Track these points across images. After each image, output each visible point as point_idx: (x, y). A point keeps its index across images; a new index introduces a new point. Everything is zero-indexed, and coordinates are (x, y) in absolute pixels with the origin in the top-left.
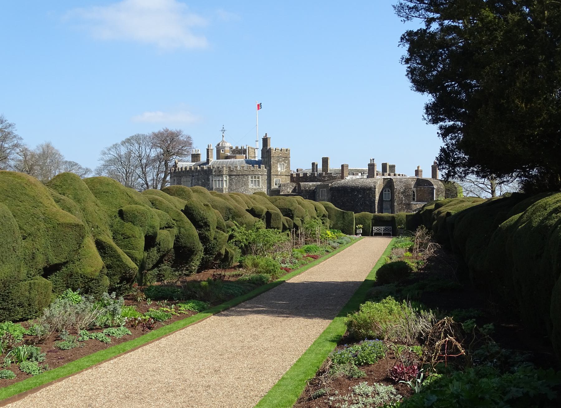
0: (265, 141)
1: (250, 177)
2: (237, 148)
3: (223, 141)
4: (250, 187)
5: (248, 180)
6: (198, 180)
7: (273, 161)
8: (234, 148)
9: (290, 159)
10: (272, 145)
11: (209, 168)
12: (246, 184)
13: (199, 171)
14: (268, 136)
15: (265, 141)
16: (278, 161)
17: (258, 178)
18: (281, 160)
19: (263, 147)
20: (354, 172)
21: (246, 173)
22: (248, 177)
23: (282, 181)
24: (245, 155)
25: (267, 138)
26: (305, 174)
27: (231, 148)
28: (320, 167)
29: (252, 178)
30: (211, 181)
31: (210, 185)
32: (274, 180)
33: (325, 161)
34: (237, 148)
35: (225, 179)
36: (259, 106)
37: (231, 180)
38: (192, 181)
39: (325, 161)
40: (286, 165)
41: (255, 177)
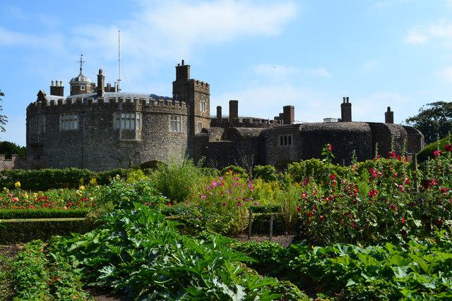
4: (170, 130)
6: (93, 118)
7: (196, 96)
9: (210, 97)
11: (112, 101)
12: (165, 127)
13: (95, 105)
22: (168, 117)
28: (226, 113)
30: (115, 121)
32: (197, 121)
33: (234, 105)
35: (138, 117)
37: (145, 120)
38: (81, 118)
39: (234, 105)
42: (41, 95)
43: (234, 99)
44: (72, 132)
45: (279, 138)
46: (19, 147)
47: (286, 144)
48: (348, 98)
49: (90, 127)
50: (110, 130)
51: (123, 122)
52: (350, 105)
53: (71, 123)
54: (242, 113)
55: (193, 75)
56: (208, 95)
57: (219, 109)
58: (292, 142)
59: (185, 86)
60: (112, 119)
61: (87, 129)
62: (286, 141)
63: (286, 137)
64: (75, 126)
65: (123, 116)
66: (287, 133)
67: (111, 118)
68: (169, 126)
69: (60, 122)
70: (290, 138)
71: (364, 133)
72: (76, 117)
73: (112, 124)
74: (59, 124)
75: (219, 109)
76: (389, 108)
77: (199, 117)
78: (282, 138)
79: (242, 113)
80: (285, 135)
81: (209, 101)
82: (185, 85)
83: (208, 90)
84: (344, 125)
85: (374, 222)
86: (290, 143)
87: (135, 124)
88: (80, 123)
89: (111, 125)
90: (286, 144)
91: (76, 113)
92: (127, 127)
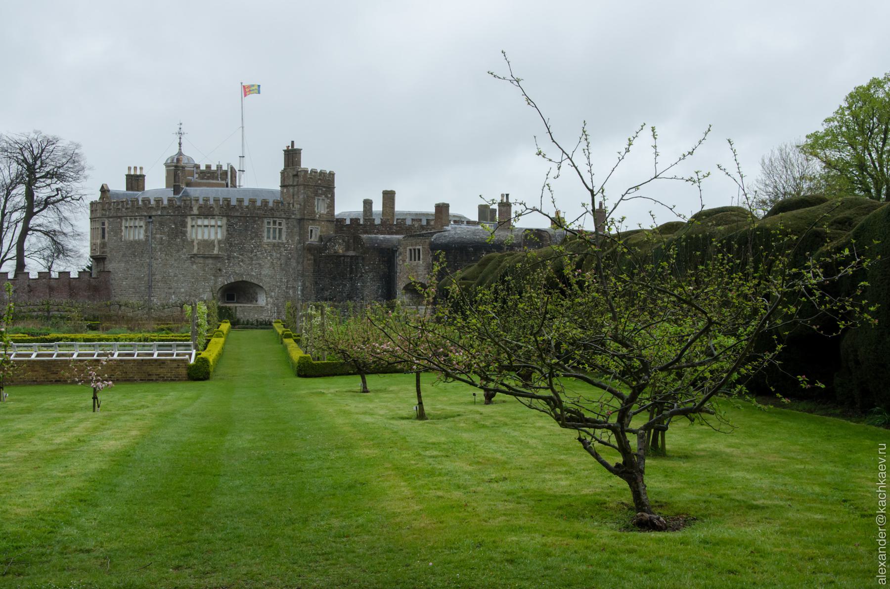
0: (292, 155)
1: (266, 221)
2: (219, 167)
3: (180, 153)
4: (265, 240)
6: (161, 224)
8: (203, 168)
9: (336, 191)
12: (257, 235)
16: (317, 194)
17: (280, 224)
18: (320, 192)
20: (459, 221)
22: (263, 222)
23: (321, 232)
24: (224, 182)
26: (355, 221)
27: (198, 167)
28: (378, 207)
29: (269, 223)
30: (189, 228)
31: (188, 235)
33: (389, 197)
34: (208, 167)
36: (247, 90)
37: (230, 226)
39: (389, 197)
44: (138, 242)
45: (408, 252)
49: (158, 236)
50: (184, 241)
53: (135, 232)
54: (402, 206)
55: (307, 163)
57: (368, 204)
60: (185, 227)
65: (200, 222)
66: (416, 245)
67: (184, 224)
68: (265, 234)
69: (123, 228)
70: (419, 250)
72: (142, 223)
73: (186, 232)
75: (368, 204)
77: (313, 220)
79: (402, 206)
85: (10, 307)
86: (419, 259)
87: (217, 233)
88: (146, 231)
89: (184, 233)
91: (141, 217)
92: (206, 237)
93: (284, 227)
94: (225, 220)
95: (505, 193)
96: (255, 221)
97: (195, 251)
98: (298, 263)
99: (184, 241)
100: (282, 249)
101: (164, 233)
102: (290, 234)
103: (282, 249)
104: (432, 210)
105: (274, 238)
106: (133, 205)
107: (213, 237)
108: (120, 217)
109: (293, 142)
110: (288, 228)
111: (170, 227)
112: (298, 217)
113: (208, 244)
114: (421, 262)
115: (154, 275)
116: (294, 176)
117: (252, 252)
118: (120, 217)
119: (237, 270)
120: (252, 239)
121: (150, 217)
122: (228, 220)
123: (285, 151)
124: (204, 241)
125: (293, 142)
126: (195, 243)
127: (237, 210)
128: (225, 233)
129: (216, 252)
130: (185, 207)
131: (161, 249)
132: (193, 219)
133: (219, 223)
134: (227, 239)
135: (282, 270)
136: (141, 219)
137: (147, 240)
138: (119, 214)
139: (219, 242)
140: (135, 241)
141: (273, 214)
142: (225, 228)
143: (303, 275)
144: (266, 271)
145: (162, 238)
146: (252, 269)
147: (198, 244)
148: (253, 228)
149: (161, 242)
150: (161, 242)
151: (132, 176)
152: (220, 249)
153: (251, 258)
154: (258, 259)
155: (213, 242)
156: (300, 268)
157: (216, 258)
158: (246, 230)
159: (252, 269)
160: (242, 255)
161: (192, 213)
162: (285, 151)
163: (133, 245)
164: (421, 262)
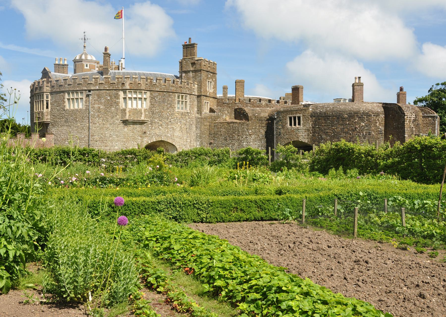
1: (177, 95)
4: (177, 110)
5: (174, 100)
6: (99, 96)
9: (218, 76)
10: (200, 54)
12: (172, 106)
14: (192, 42)
15: (189, 48)
16: (208, 78)
18: (209, 76)
19: (185, 55)
21: (173, 89)
22: (175, 96)
23: (210, 105)
25: (194, 44)
30: (121, 100)
31: (120, 105)
33: (240, 84)
37: (152, 98)
39: (240, 84)
40: (213, 83)
41: (182, 96)
42: (45, 74)
43: (239, 78)
46: (19, 125)
47: (295, 125)
48: (359, 78)
49: (96, 106)
50: (117, 109)
51: (129, 102)
52: (362, 85)
56: (214, 73)
57: (225, 88)
58: (302, 122)
59: (192, 66)
60: (118, 98)
61: (93, 107)
62: (295, 120)
63: (295, 118)
64: (80, 106)
67: (117, 97)
68: (176, 106)
69: (66, 100)
70: (299, 118)
71: (377, 114)
74: (64, 102)
76: (401, 89)
77: (206, 96)
78: (290, 118)
80: (294, 115)
81: (216, 80)
82: (192, 63)
83: (215, 69)
84: (355, 106)
86: (299, 124)
89: (118, 104)
90: (295, 125)
92: (134, 106)
93: (188, 100)
94: (148, 93)
95: (357, 76)
96: (170, 95)
97: (127, 118)
98: (197, 127)
99: (117, 109)
100: (187, 117)
101: (101, 103)
102: (192, 107)
103: (187, 117)
104: (290, 91)
105: (182, 108)
106: (75, 82)
107: (139, 107)
108: (63, 92)
109: (190, 38)
110: (190, 101)
111: (106, 99)
112: (196, 94)
113: (137, 112)
114: (302, 126)
115: (92, 136)
116: (192, 63)
117: (168, 119)
118: (63, 92)
119: (157, 131)
120: (168, 109)
121: (90, 91)
122: (151, 94)
123: (184, 46)
124: (134, 109)
125: (190, 38)
126: (127, 111)
127: (158, 87)
128: (149, 104)
129: (143, 118)
130: (118, 83)
131: (98, 116)
132: (125, 93)
133: (145, 96)
134: (150, 108)
135: (187, 133)
136: (81, 93)
137: (87, 109)
138: (63, 90)
139: (145, 110)
140: (77, 110)
141: (181, 91)
142: (148, 100)
143: (201, 137)
144: (177, 133)
145: (99, 108)
146: (168, 132)
147: (129, 112)
148: (168, 100)
149: (99, 110)
150: (99, 110)
151: (59, 65)
152: (145, 115)
153: (167, 123)
154: (172, 124)
155: (140, 111)
156: (198, 131)
157: (142, 123)
158: (164, 102)
159: (168, 132)
160: (161, 121)
161: (124, 88)
162: (184, 46)
163: (74, 112)
164: (302, 126)
